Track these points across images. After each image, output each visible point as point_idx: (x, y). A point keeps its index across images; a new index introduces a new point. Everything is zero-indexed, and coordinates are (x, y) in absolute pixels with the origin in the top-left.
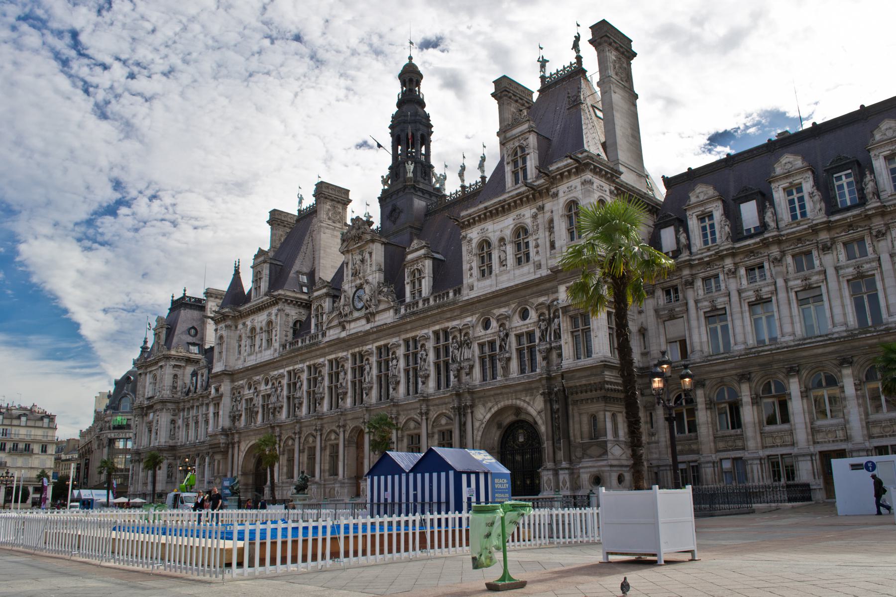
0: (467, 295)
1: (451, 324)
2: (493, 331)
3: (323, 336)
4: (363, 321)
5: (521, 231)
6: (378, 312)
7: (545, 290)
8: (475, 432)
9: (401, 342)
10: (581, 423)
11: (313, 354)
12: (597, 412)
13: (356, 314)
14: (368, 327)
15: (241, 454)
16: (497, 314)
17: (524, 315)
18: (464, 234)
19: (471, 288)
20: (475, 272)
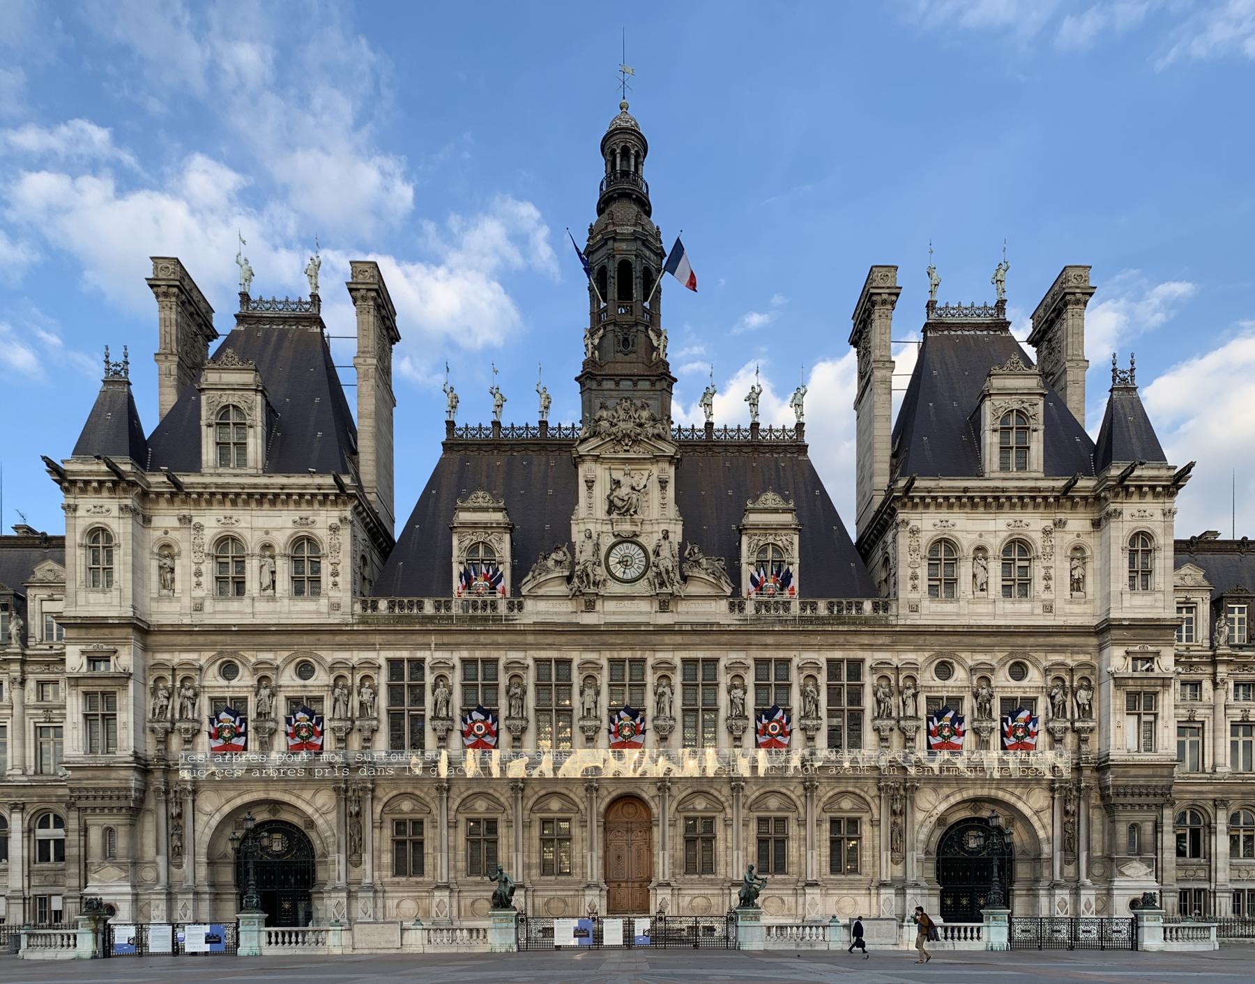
0: (902, 616)
1: (870, 658)
2: (959, 684)
3: (511, 609)
4: (644, 606)
5: (1018, 547)
6: (689, 597)
7: (1061, 646)
8: (917, 827)
9: (751, 663)
10: (1112, 834)
11: (482, 638)
12: (1142, 822)
13: (614, 588)
14: (665, 619)
15: (202, 819)
16: (970, 663)
17: (1018, 671)
18: (901, 516)
19: (914, 609)
20: (923, 583)
